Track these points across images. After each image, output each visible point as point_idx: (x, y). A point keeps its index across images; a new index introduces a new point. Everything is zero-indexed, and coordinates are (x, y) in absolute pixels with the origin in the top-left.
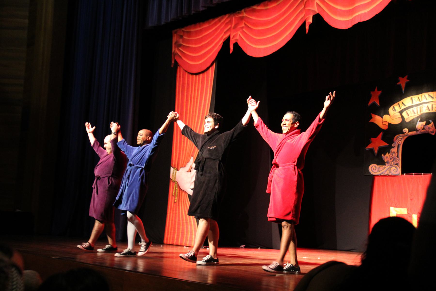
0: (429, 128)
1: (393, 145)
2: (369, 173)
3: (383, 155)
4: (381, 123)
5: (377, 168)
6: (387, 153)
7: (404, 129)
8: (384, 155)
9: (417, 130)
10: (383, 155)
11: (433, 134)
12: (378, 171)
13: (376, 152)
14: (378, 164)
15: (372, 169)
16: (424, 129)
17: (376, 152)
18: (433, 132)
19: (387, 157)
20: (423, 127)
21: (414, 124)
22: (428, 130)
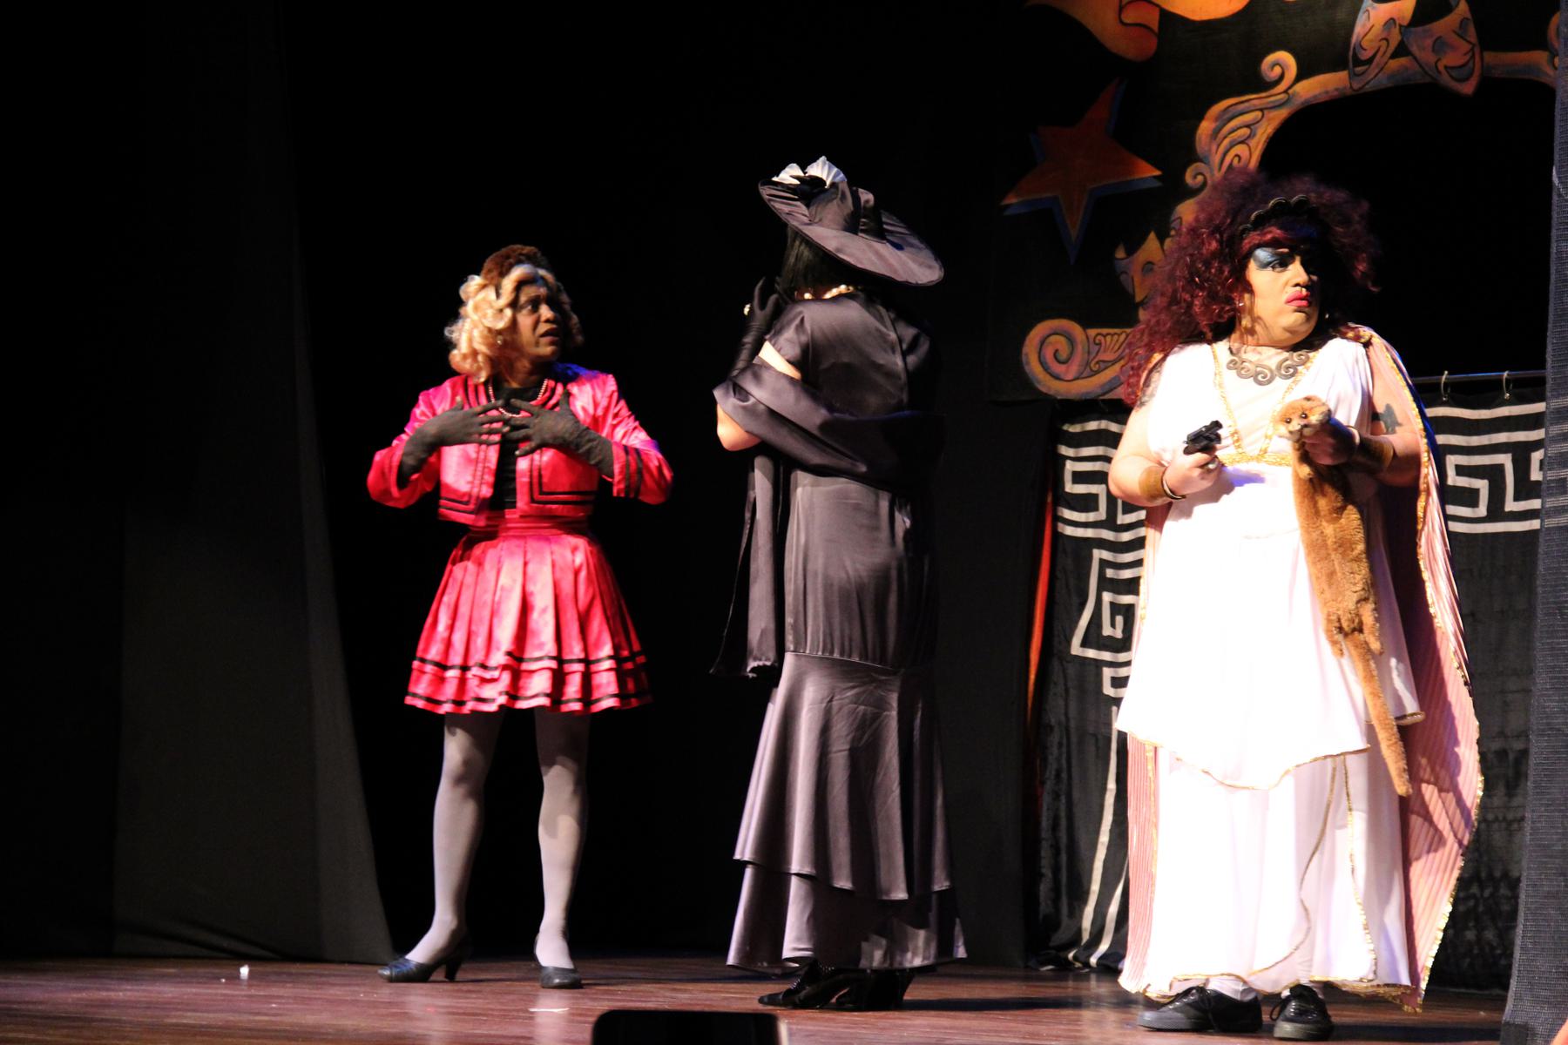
0: (1439, 46)
1: (1189, 178)
2: (1026, 382)
3: (1120, 254)
4: (1110, 16)
5: (1079, 349)
6: (1152, 241)
7: (1271, 58)
8: (1131, 251)
9: (1358, 62)
10: (1120, 254)
11: (1468, 88)
12: (1088, 371)
13: (1074, 229)
14: (1086, 324)
15: (1048, 354)
16: (1401, 50)
17: (1074, 229)
18: (1461, 72)
19: (1148, 266)
20: (1395, 38)
21: (1341, 15)
22: (1428, 57)
